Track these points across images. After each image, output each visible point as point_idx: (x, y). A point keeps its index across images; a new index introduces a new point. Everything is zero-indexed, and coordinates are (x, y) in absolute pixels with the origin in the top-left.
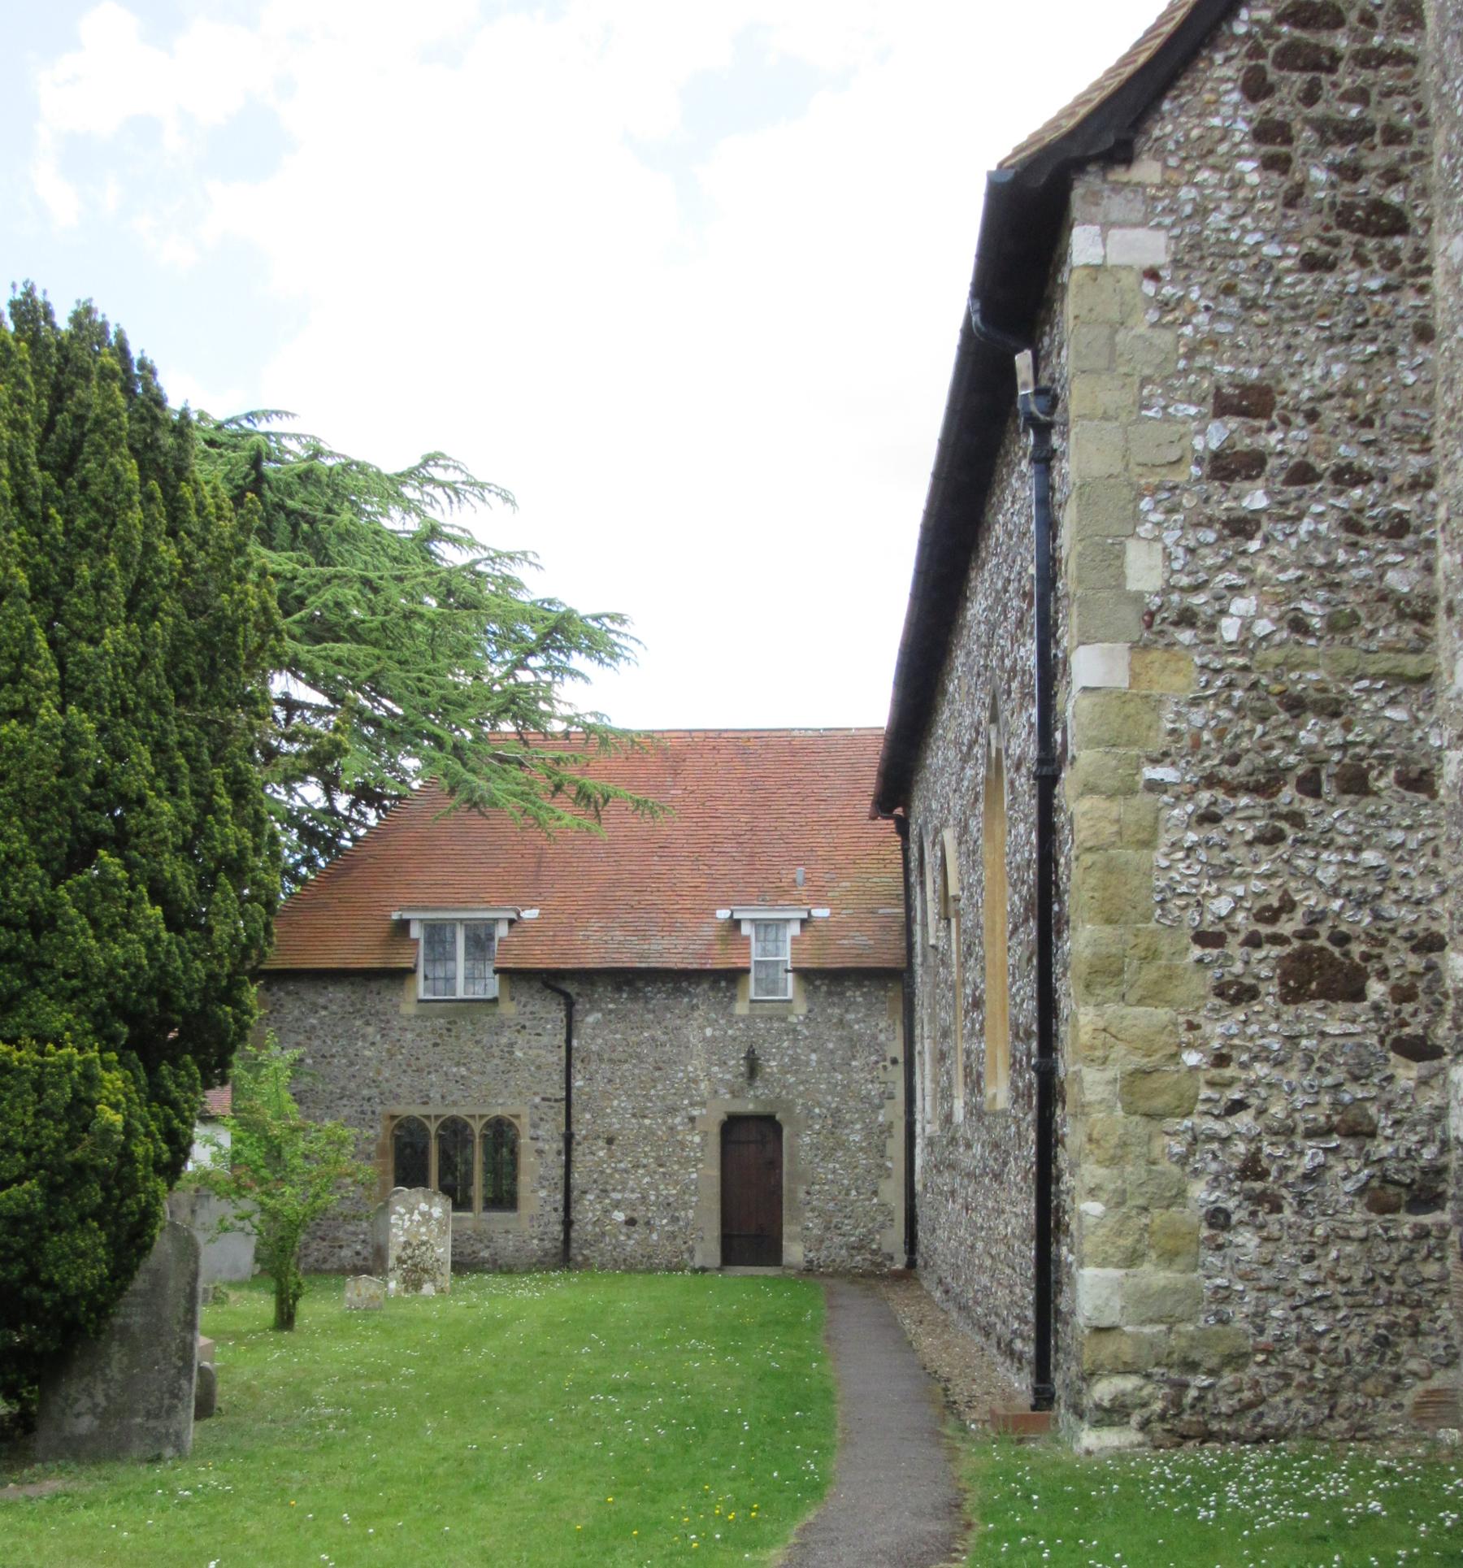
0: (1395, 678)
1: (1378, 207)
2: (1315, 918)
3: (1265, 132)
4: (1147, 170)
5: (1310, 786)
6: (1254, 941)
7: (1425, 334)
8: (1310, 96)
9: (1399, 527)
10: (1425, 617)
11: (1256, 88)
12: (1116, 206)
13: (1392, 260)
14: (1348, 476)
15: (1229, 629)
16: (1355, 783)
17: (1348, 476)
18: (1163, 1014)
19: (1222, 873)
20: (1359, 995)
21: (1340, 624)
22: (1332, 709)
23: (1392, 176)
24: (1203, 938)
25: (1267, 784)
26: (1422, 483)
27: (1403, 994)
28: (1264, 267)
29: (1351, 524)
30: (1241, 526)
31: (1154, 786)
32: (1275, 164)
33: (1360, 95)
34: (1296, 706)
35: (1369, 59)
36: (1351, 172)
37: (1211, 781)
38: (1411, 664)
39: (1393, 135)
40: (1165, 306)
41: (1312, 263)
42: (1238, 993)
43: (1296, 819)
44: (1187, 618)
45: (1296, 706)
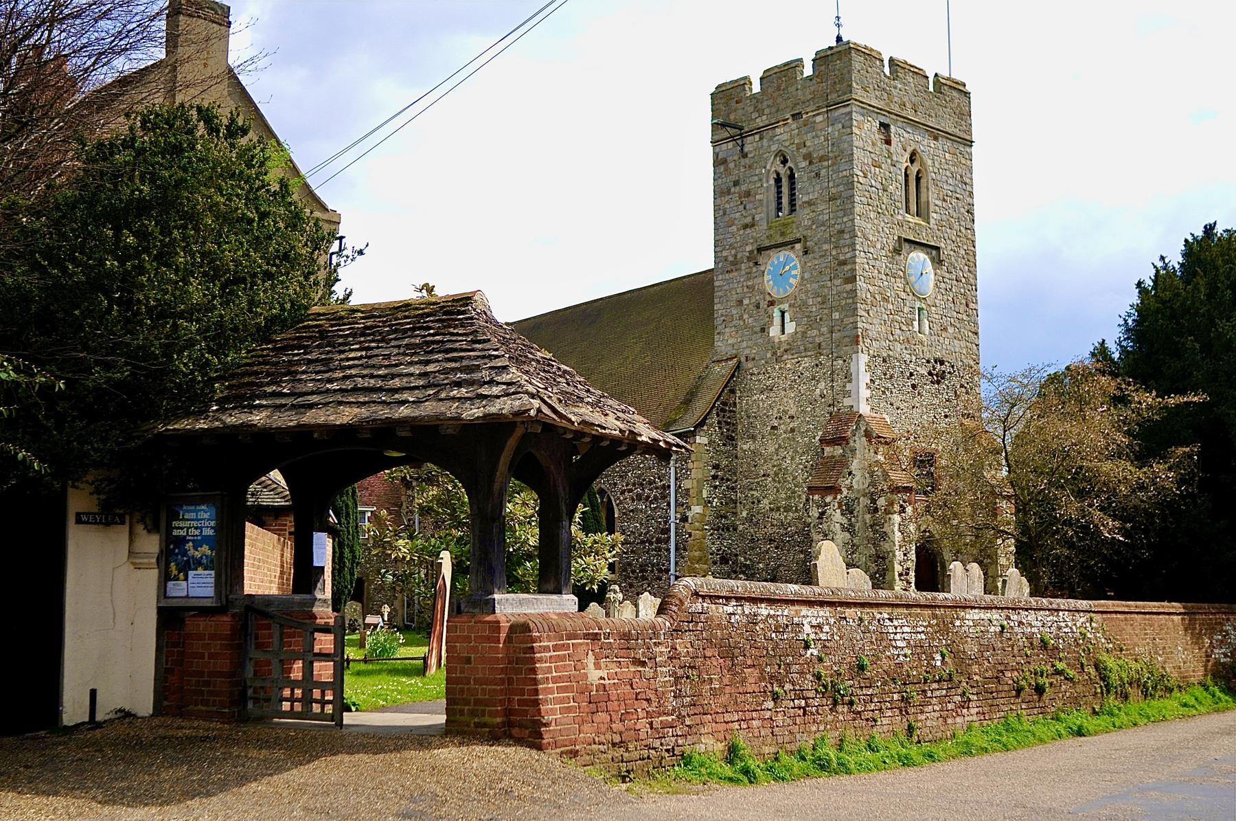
0: (733, 513)
1: (731, 436)
2: (724, 551)
3: (719, 422)
4: (705, 428)
5: (723, 530)
6: (717, 555)
7: (736, 457)
8: (724, 417)
9: (733, 488)
10: (736, 503)
11: (718, 415)
12: (702, 433)
13: (733, 445)
14: (728, 480)
15: (714, 504)
16: (728, 530)
17: (728, 480)
18: (706, 566)
19: (713, 543)
20: (728, 563)
21: (726, 504)
22: (726, 517)
23: (733, 432)
24: (711, 554)
25: (718, 530)
26: (736, 482)
27: (733, 563)
28: (719, 445)
29: (727, 488)
30: (716, 487)
31: (706, 529)
32: (720, 428)
33: (729, 418)
34: (722, 517)
35: (730, 411)
36: (728, 430)
37: (712, 529)
38: (734, 510)
39: (733, 425)
40: (708, 450)
41: (724, 445)
42: (714, 563)
43: (721, 535)
44: (709, 502)
45: (722, 517)
